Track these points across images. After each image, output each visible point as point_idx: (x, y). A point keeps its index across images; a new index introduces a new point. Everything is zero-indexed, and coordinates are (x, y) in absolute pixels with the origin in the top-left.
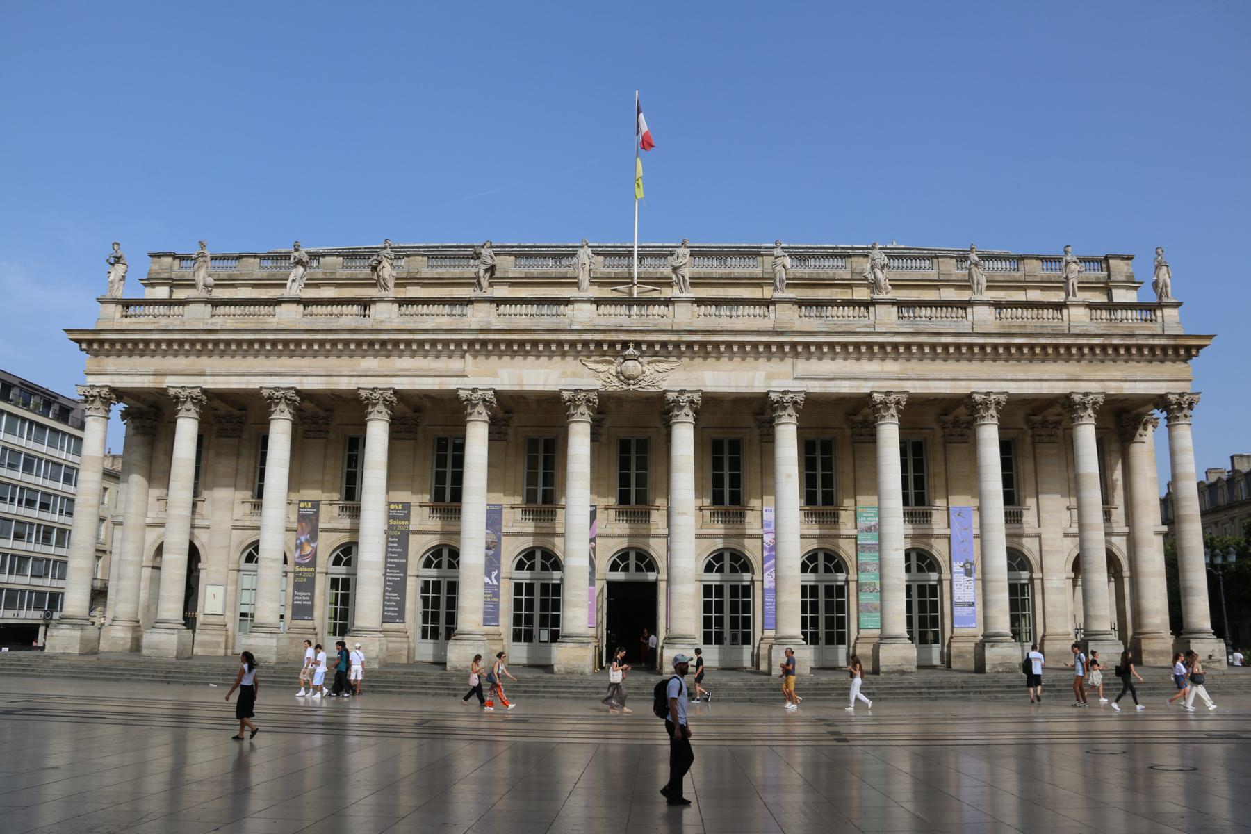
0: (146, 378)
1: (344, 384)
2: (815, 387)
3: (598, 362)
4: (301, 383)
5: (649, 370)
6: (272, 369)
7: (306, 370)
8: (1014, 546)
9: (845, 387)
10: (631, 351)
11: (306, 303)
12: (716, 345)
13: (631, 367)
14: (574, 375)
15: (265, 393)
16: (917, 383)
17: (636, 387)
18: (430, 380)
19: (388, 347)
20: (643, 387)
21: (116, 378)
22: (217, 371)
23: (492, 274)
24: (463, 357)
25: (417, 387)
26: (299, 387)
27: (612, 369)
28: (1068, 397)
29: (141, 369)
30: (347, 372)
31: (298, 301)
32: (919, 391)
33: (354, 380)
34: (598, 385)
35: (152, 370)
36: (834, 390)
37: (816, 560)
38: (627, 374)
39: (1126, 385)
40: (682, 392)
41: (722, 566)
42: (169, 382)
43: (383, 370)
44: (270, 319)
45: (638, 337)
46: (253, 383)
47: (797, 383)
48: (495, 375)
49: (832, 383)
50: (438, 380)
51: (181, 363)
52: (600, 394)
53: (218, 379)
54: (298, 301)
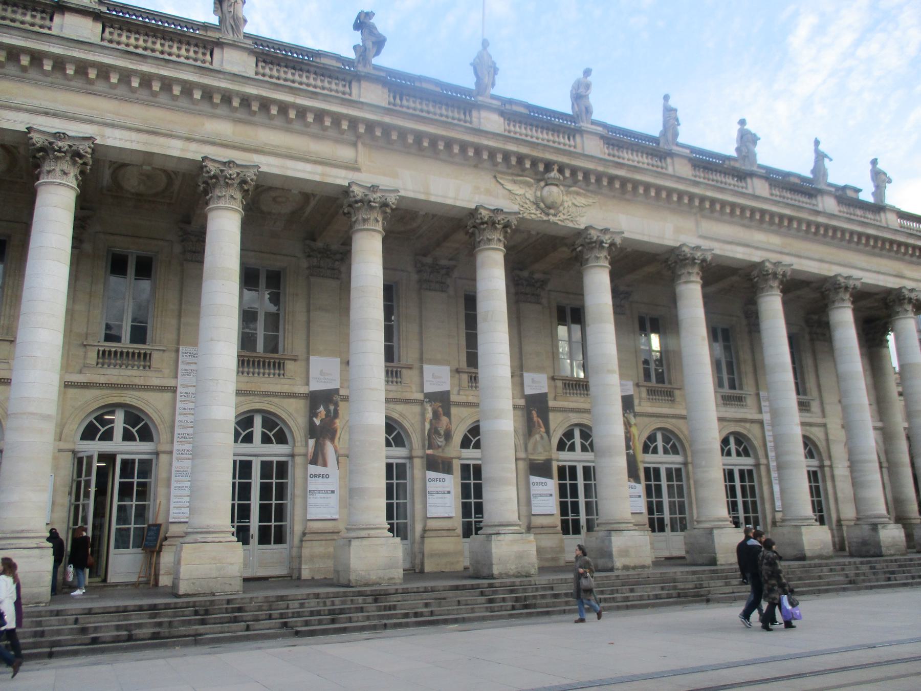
3: (515, 182)
4: (103, 136)
5: (568, 201)
7: (110, 118)
8: (808, 434)
10: (554, 174)
12: (636, 184)
13: (554, 193)
15: (36, 138)
18: (308, 167)
24: (355, 145)
25: (290, 173)
27: (530, 194)
36: (731, 254)
37: (655, 441)
38: (549, 201)
40: (605, 231)
41: (573, 444)
45: (564, 160)
49: (729, 247)
50: (319, 169)
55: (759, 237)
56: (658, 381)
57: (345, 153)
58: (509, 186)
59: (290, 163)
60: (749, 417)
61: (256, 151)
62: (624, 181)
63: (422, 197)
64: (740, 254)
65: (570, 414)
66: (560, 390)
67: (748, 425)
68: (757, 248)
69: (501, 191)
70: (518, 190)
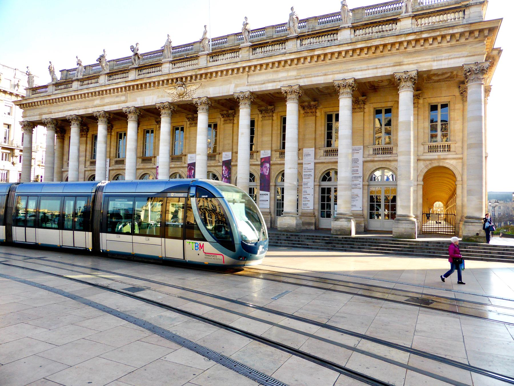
1: (90, 111)
2: (256, 88)
10: (179, 82)
14: (162, 96)
16: (305, 80)
17: (183, 99)
19: (100, 93)
20: (186, 98)
21: (30, 118)
25: (112, 109)
28: (393, 76)
32: (307, 84)
34: (170, 100)
36: (264, 89)
43: (101, 103)
48: (136, 100)
49: (264, 85)
50: (118, 105)
52: (170, 104)
55: (282, 75)
57: (123, 98)
58: (169, 91)
59: (112, 106)
61: (104, 105)
63: (143, 105)
64: (270, 87)
68: (280, 81)
70: (171, 91)
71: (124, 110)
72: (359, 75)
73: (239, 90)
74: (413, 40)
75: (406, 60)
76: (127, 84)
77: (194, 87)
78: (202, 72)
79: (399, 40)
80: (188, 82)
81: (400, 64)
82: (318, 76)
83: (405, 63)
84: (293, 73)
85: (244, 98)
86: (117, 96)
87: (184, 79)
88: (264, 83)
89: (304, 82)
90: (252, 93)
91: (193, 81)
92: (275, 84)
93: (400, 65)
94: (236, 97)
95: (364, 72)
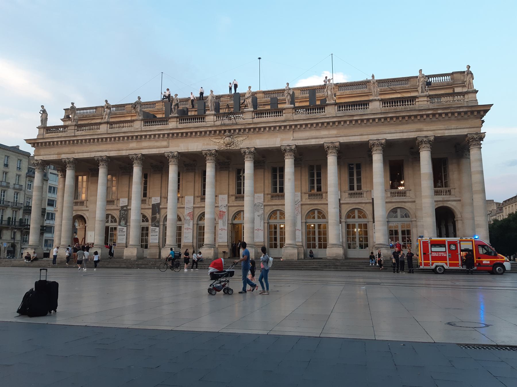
0: (55, 156)
1: (124, 153)
2: (301, 143)
6: (99, 149)
7: (111, 149)
9: (313, 142)
10: (227, 133)
11: (111, 124)
12: (260, 128)
14: (207, 144)
16: (344, 138)
17: (230, 148)
18: (155, 150)
19: (138, 138)
20: (233, 147)
21: (44, 157)
22: (79, 151)
23: (178, 107)
26: (108, 155)
27: (222, 141)
28: (416, 139)
29: (52, 153)
30: (125, 149)
31: (107, 123)
33: (128, 151)
34: (217, 148)
35: (56, 152)
39: (447, 131)
40: (248, 148)
42: (63, 156)
43: (138, 147)
44: (98, 130)
45: (229, 128)
46: (92, 155)
47: (293, 142)
49: (308, 141)
50: (158, 150)
51: (66, 149)
53: (80, 154)
54: (107, 123)
55: (324, 133)
56: (318, 190)
57: (165, 143)
58: (215, 140)
59: (150, 150)
60: (363, 201)
62: (255, 129)
65: (274, 207)
66: (270, 199)
67: (363, 205)
68: (322, 138)
69: (212, 143)
71: (166, 154)
72: (389, 137)
73: (285, 143)
74: (431, 114)
75: (425, 128)
76: (171, 132)
77: (241, 139)
78: (252, 126)
79: (421, 113)
80: (236, 133)
81: (421, 130)
82: (355, 136)
83: (425, 129)
84: (334, 132)
85: (291, 150)
86: (157, 141)
87: (232, 131)
88: (308, 139)
89: (343, 140)
90: (297, 146)
91: (241, 133)
92: (318, 140)
93: (420, 131)
94: (283, 148)
95: (392, 135)
